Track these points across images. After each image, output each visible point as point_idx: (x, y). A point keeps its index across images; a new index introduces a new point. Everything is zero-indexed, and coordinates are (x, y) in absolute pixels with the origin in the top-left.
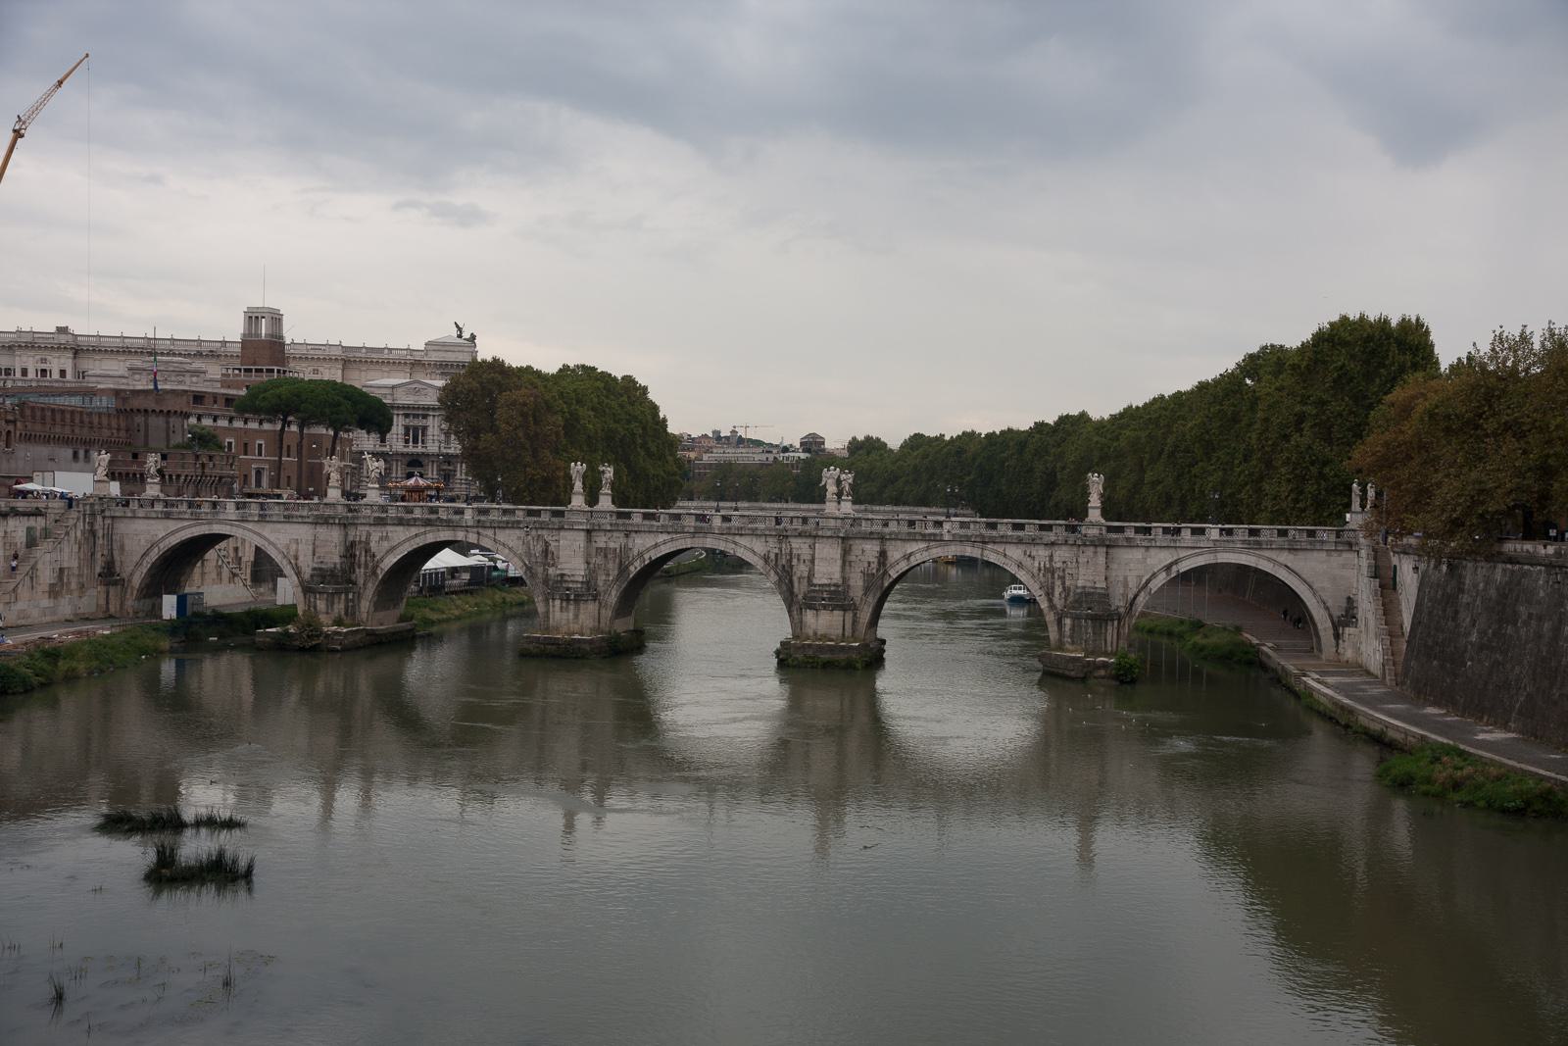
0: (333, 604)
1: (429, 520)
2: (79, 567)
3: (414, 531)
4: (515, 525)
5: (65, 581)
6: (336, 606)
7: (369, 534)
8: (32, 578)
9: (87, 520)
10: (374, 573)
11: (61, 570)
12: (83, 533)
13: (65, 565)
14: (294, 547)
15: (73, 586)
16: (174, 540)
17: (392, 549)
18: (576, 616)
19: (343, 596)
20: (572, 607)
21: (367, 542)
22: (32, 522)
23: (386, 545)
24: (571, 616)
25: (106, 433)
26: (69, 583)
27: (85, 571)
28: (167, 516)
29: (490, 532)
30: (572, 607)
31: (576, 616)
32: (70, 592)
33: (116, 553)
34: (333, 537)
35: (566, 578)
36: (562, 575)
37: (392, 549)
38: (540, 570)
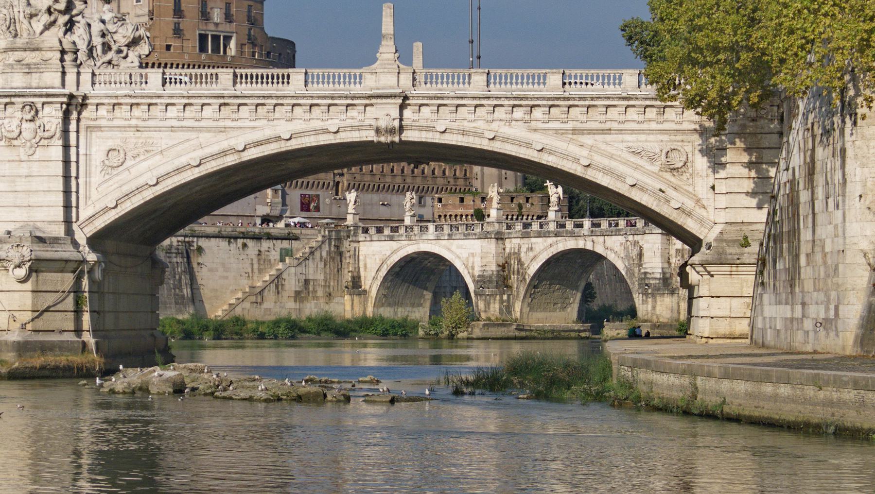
0: (489, 304)
1: (559, 232)
2: (325, 280)
3: (550, 240)
4: (618, 233)
5: (311, 289)
6: (492, 306)
7: (520, 247)
8: (277, 287)
9: (333, 243)
10: (524, 279)
11: (307, 281)
12: (329, 253)
13: (311, 277)
14: (471, 259)
15: (320, 293)
16: (396, 258)
17: (535, 257)
18: (654, 308)
19: (498, 298)
20: (650, 300)
21: (519, 254)
22: (286, 244)
23: (531, 254)
24: (650, 308)
25: (440, 181)
26: (315, 291)
27: (332, 284)
28: (391, 239)
29: (601, 239)
30: (650, 300)
31: (654, 308)
32: (316, 298)
33: (362, 270)
34: (491, 246)
35: (648, 276)
36: (645, 273)
37: (535, 257)
38: (636, 270)
